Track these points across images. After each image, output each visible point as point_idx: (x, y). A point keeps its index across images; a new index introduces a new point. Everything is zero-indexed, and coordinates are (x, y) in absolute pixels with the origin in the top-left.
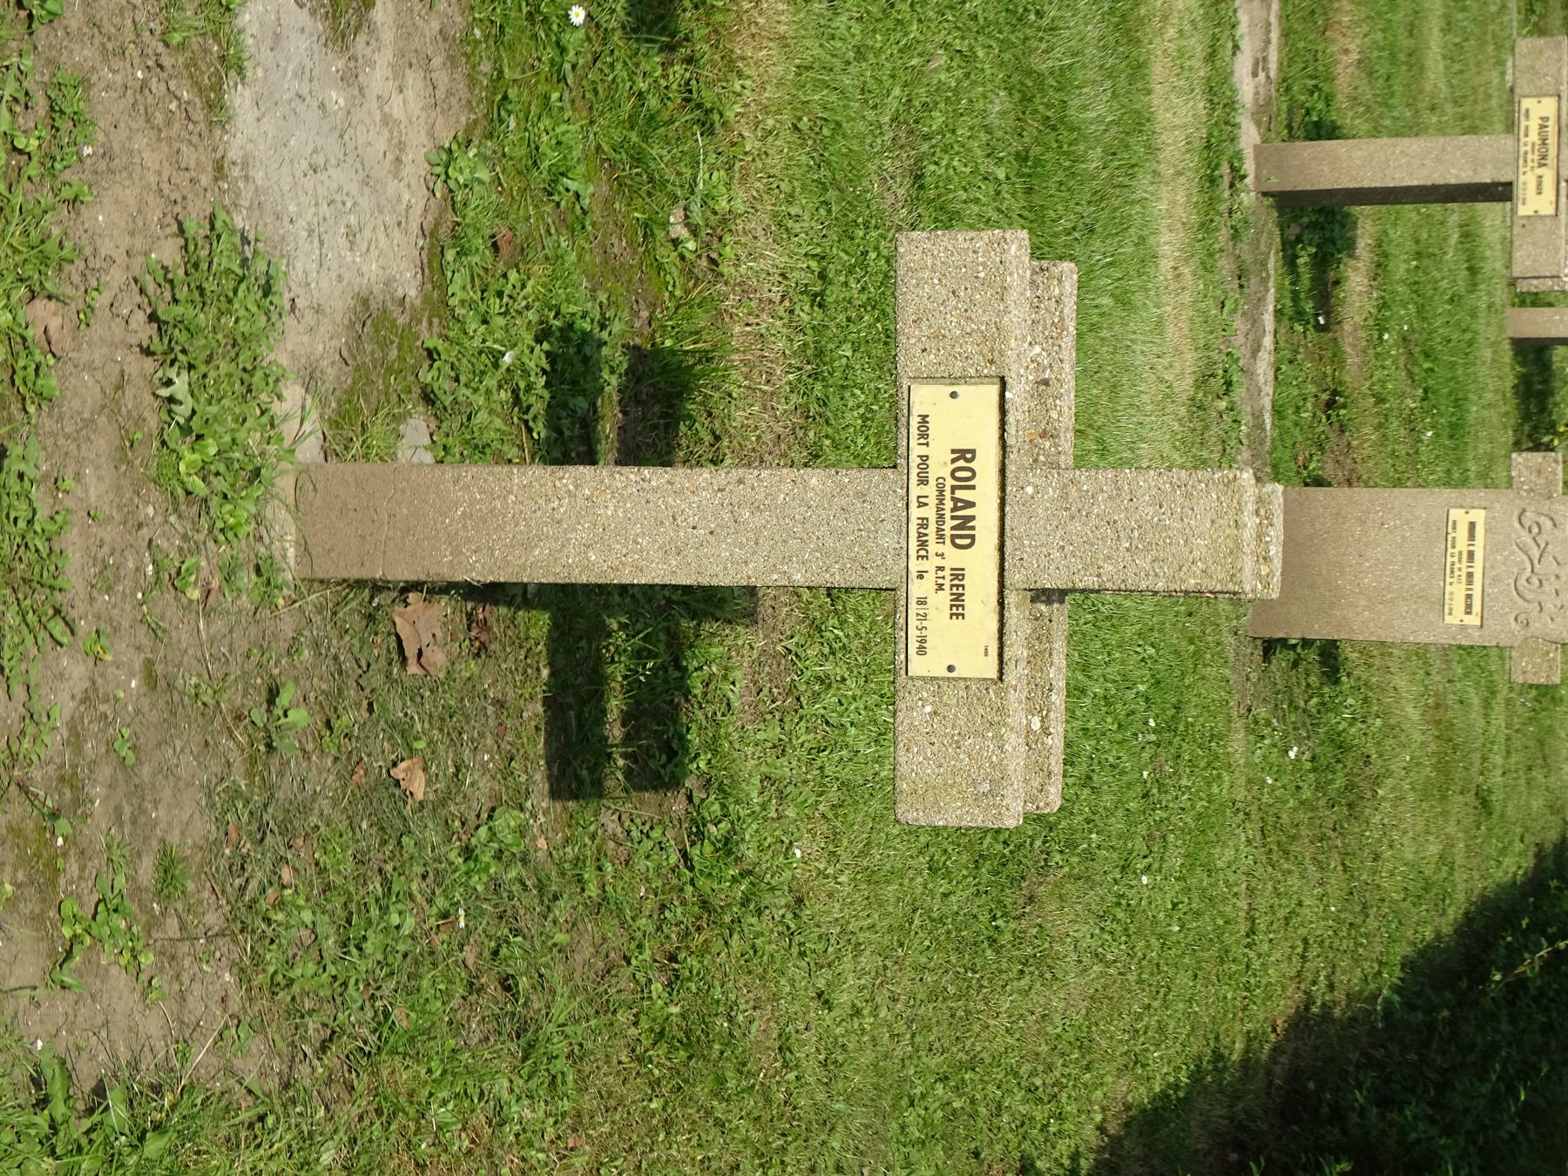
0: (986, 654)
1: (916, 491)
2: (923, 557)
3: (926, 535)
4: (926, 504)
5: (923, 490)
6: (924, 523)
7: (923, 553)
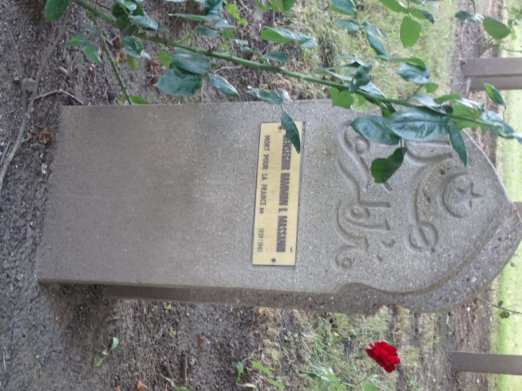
0: (291, 252)
1: (261, 171)
2: (263, 204)
3: (265, 193)
4: (266, 178)
5: (265, 171)
6: (265, 188)
7: (263, 202)
